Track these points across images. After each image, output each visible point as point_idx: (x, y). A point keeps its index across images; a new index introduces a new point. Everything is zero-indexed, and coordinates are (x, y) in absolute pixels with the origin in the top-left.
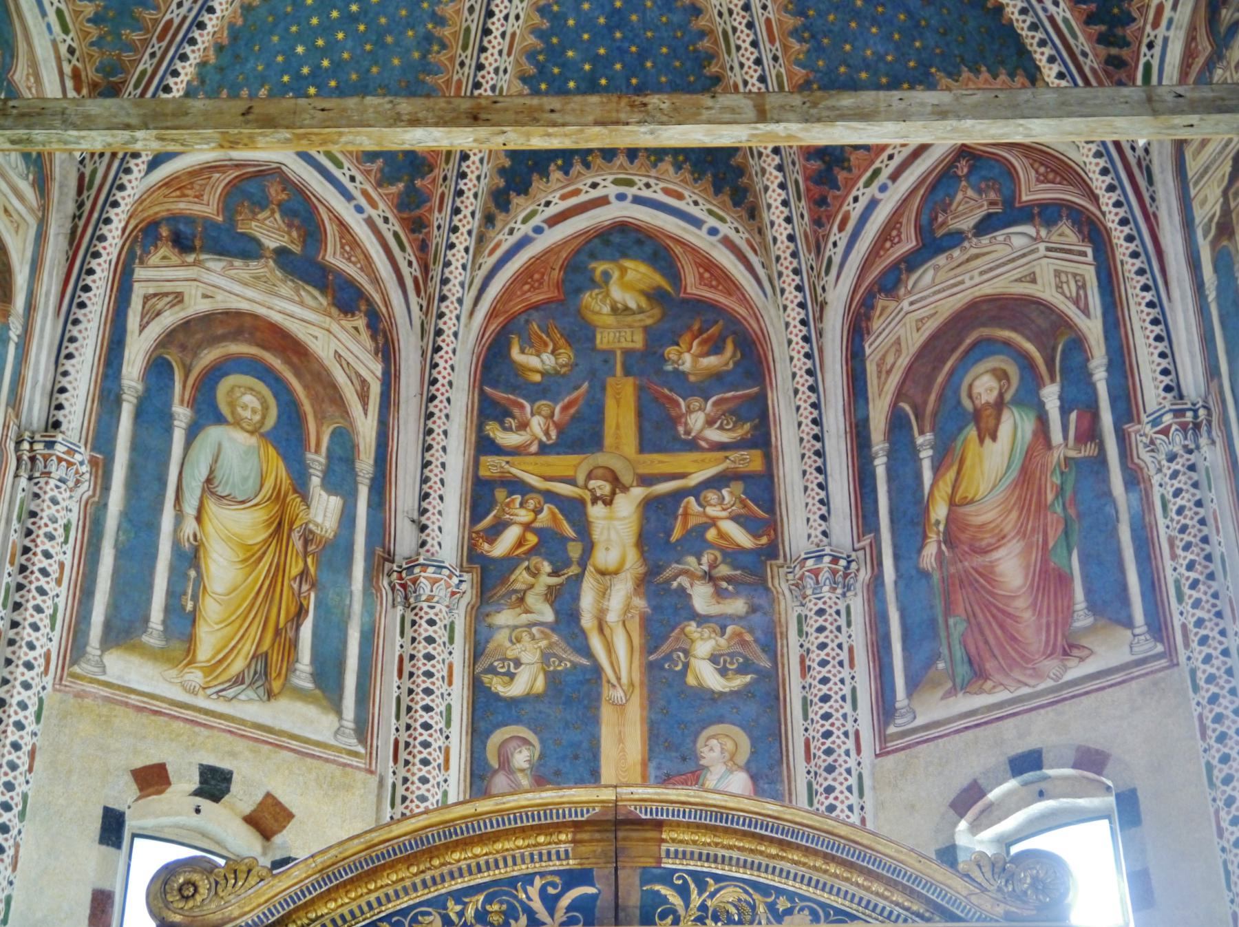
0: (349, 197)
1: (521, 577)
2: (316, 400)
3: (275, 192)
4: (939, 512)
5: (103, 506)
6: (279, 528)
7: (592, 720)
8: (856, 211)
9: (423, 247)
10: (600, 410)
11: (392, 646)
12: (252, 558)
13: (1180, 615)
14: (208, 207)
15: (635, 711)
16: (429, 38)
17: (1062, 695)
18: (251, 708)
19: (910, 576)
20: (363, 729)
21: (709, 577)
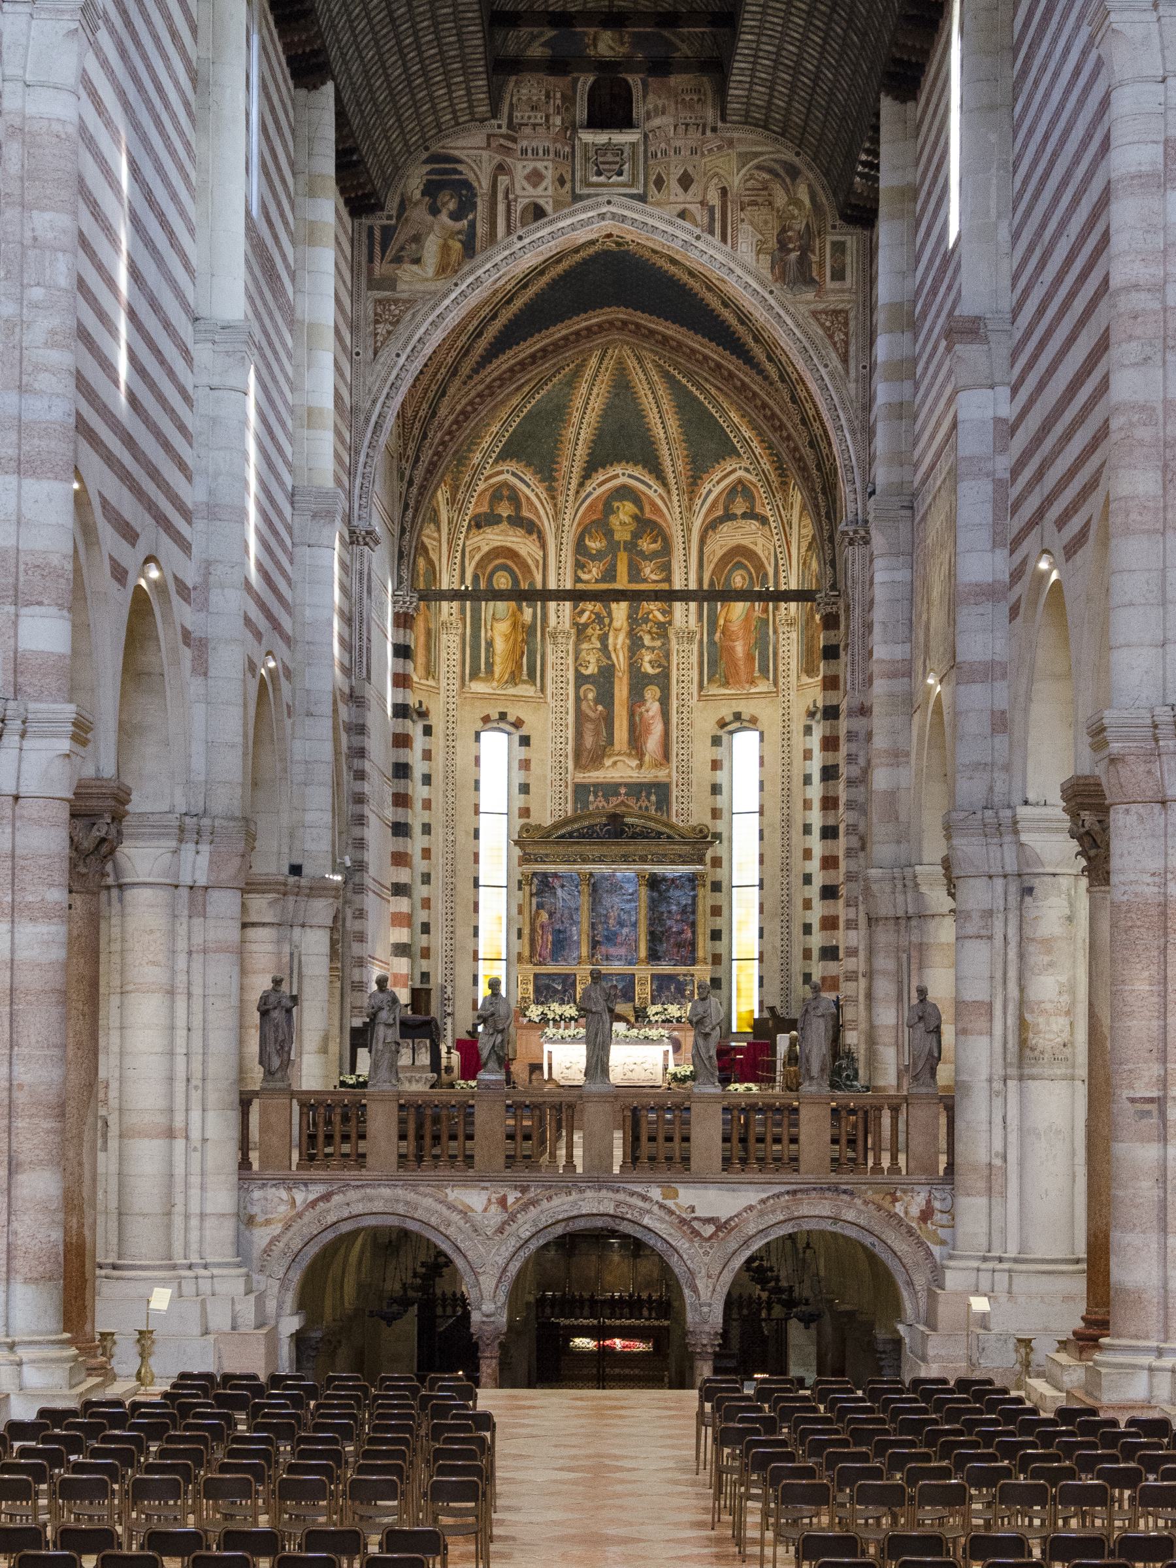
0: (528, 486)
1: (589, 631)
2: (523, 574)
3: (506, 493)
4: (721, 622)
5: (464, 634)
6: (514, 625)
7: (612, 684)
8: (704, 492)
9: (555, 505)
10: (615, 566)
11: (550, 659)
12: (507, 638)
13: (781, 680)
14: (485, 508)
15: (625, 680)
16: (557, 441)
17: (748, 696)
18: (512, 691)
19: (712, 643)
20: (543, 690)
21: (649, 632)
